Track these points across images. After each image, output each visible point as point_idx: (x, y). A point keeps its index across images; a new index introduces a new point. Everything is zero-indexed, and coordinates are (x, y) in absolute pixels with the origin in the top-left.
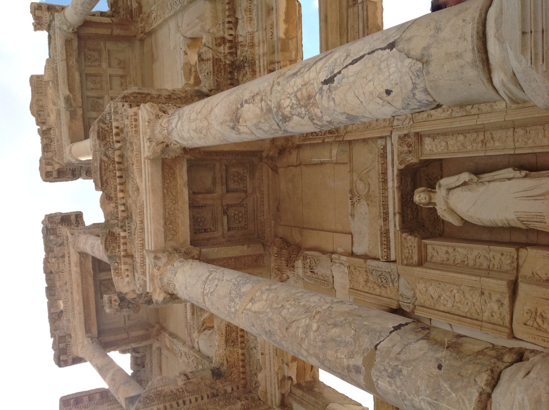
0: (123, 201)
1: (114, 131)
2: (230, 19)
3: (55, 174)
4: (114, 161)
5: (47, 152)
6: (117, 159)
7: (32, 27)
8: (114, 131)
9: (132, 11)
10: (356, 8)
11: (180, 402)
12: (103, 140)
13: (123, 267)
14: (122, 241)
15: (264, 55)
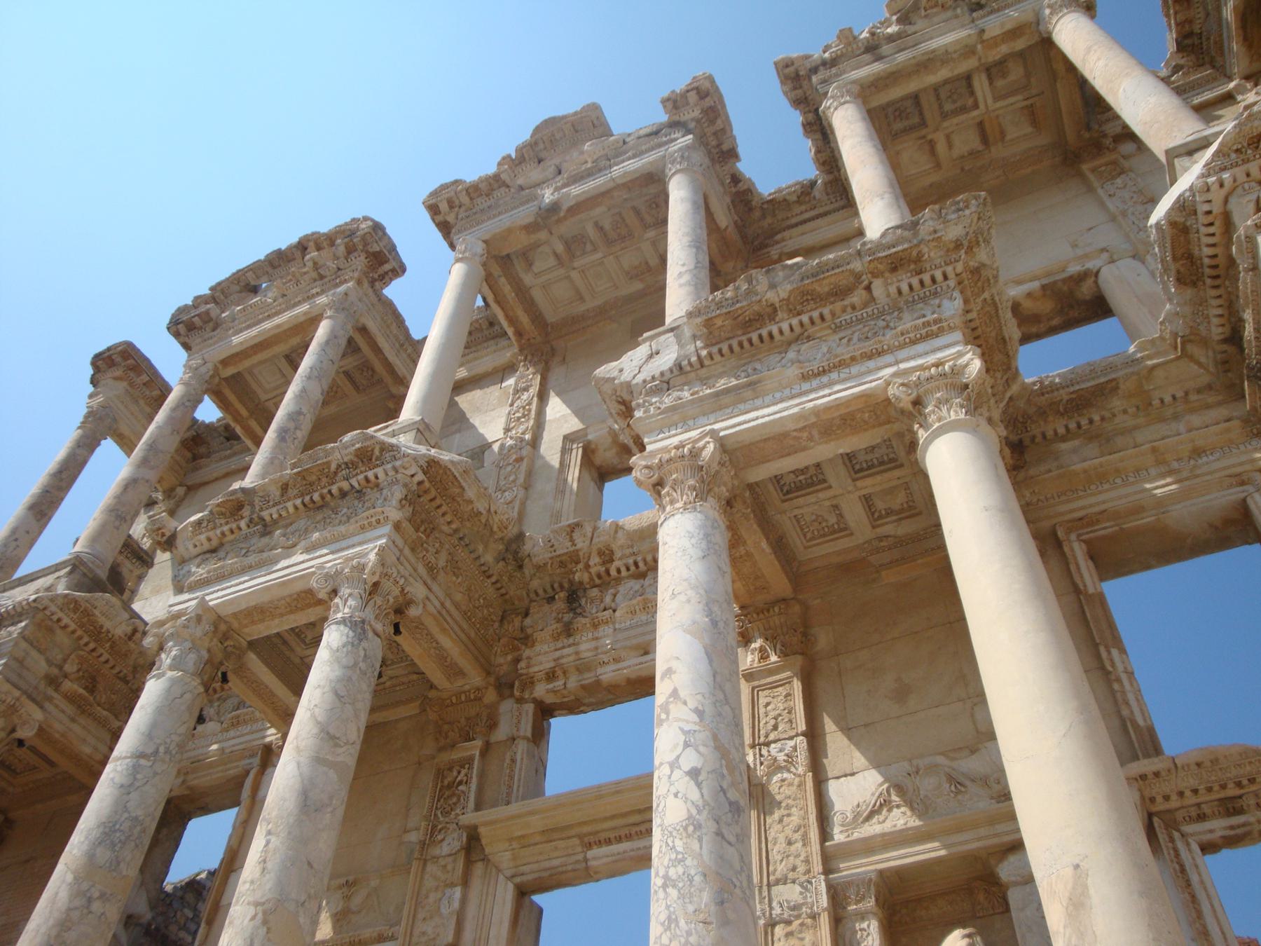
0: (284, 514)
1: (370, 474)
2: (641, 564)
3: (439, 218)
4: (333, 483)
5: (468, 193)
6: (334, 489)
7: (666, 94)
8: (370, 474)
9: (766, 246)
10: (580, 849)
11: (92, 646)
12: (357, 456)
13: (203, 537)
14: (234, 526)
15: (577, 653)
